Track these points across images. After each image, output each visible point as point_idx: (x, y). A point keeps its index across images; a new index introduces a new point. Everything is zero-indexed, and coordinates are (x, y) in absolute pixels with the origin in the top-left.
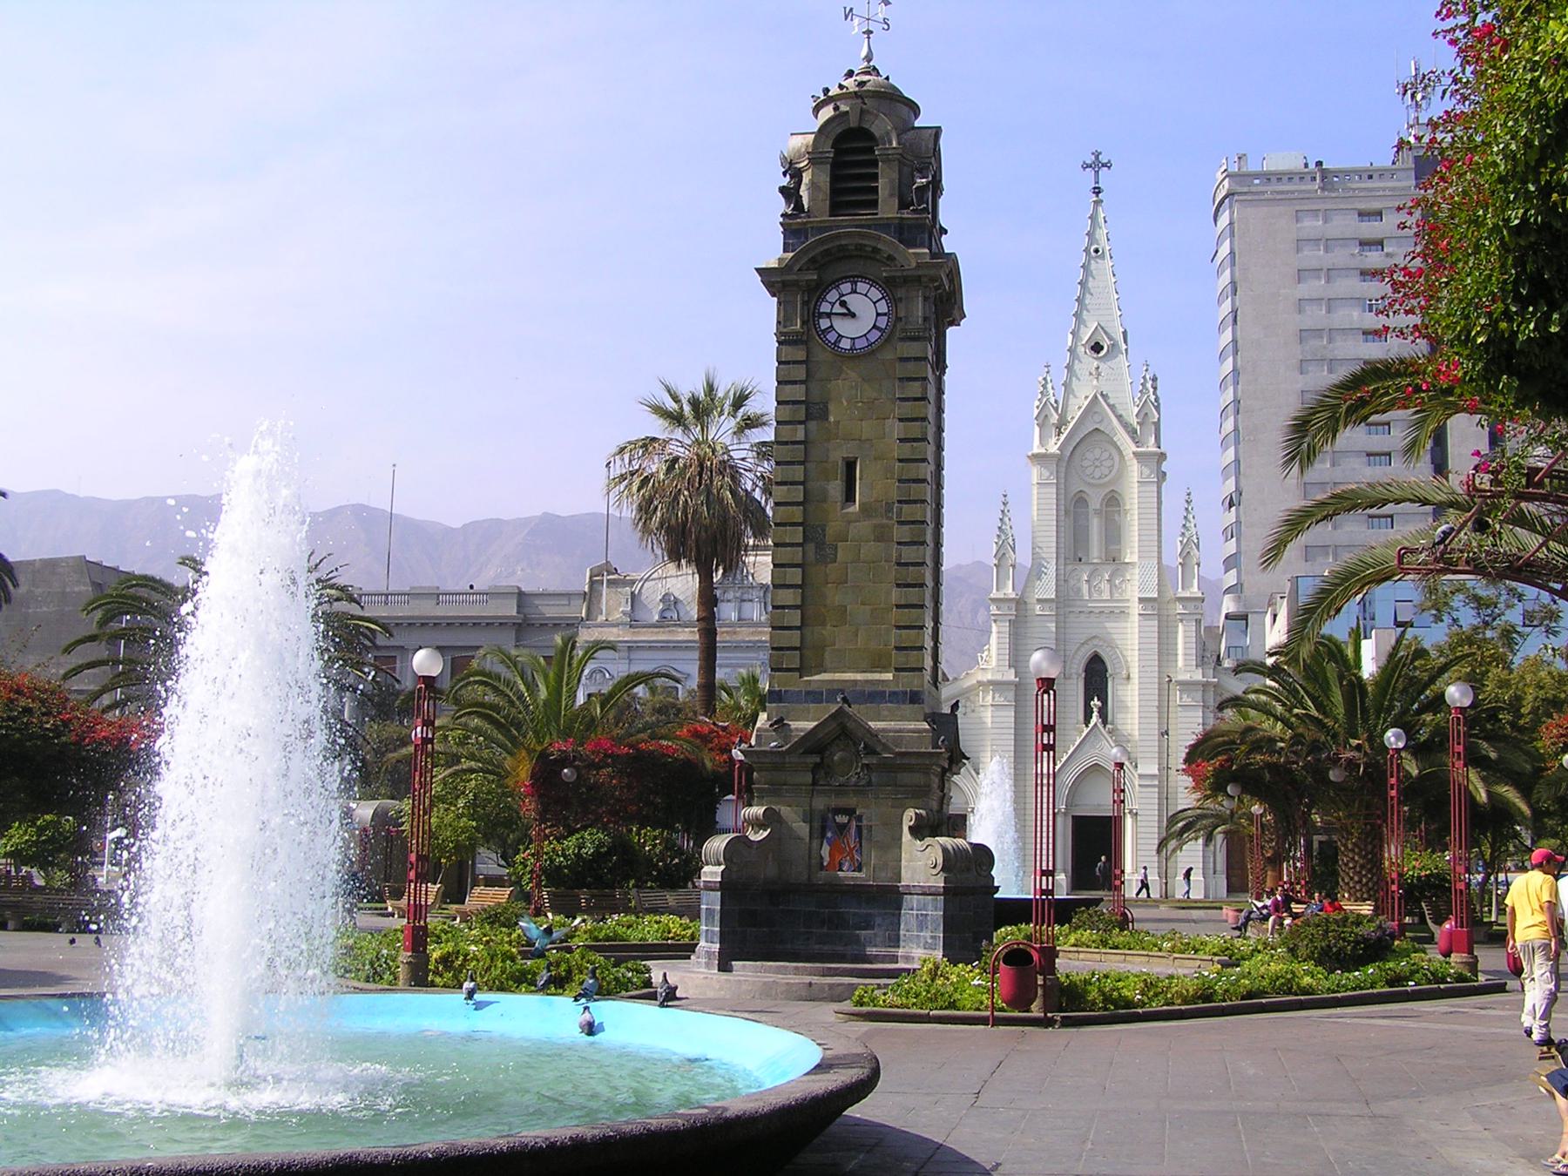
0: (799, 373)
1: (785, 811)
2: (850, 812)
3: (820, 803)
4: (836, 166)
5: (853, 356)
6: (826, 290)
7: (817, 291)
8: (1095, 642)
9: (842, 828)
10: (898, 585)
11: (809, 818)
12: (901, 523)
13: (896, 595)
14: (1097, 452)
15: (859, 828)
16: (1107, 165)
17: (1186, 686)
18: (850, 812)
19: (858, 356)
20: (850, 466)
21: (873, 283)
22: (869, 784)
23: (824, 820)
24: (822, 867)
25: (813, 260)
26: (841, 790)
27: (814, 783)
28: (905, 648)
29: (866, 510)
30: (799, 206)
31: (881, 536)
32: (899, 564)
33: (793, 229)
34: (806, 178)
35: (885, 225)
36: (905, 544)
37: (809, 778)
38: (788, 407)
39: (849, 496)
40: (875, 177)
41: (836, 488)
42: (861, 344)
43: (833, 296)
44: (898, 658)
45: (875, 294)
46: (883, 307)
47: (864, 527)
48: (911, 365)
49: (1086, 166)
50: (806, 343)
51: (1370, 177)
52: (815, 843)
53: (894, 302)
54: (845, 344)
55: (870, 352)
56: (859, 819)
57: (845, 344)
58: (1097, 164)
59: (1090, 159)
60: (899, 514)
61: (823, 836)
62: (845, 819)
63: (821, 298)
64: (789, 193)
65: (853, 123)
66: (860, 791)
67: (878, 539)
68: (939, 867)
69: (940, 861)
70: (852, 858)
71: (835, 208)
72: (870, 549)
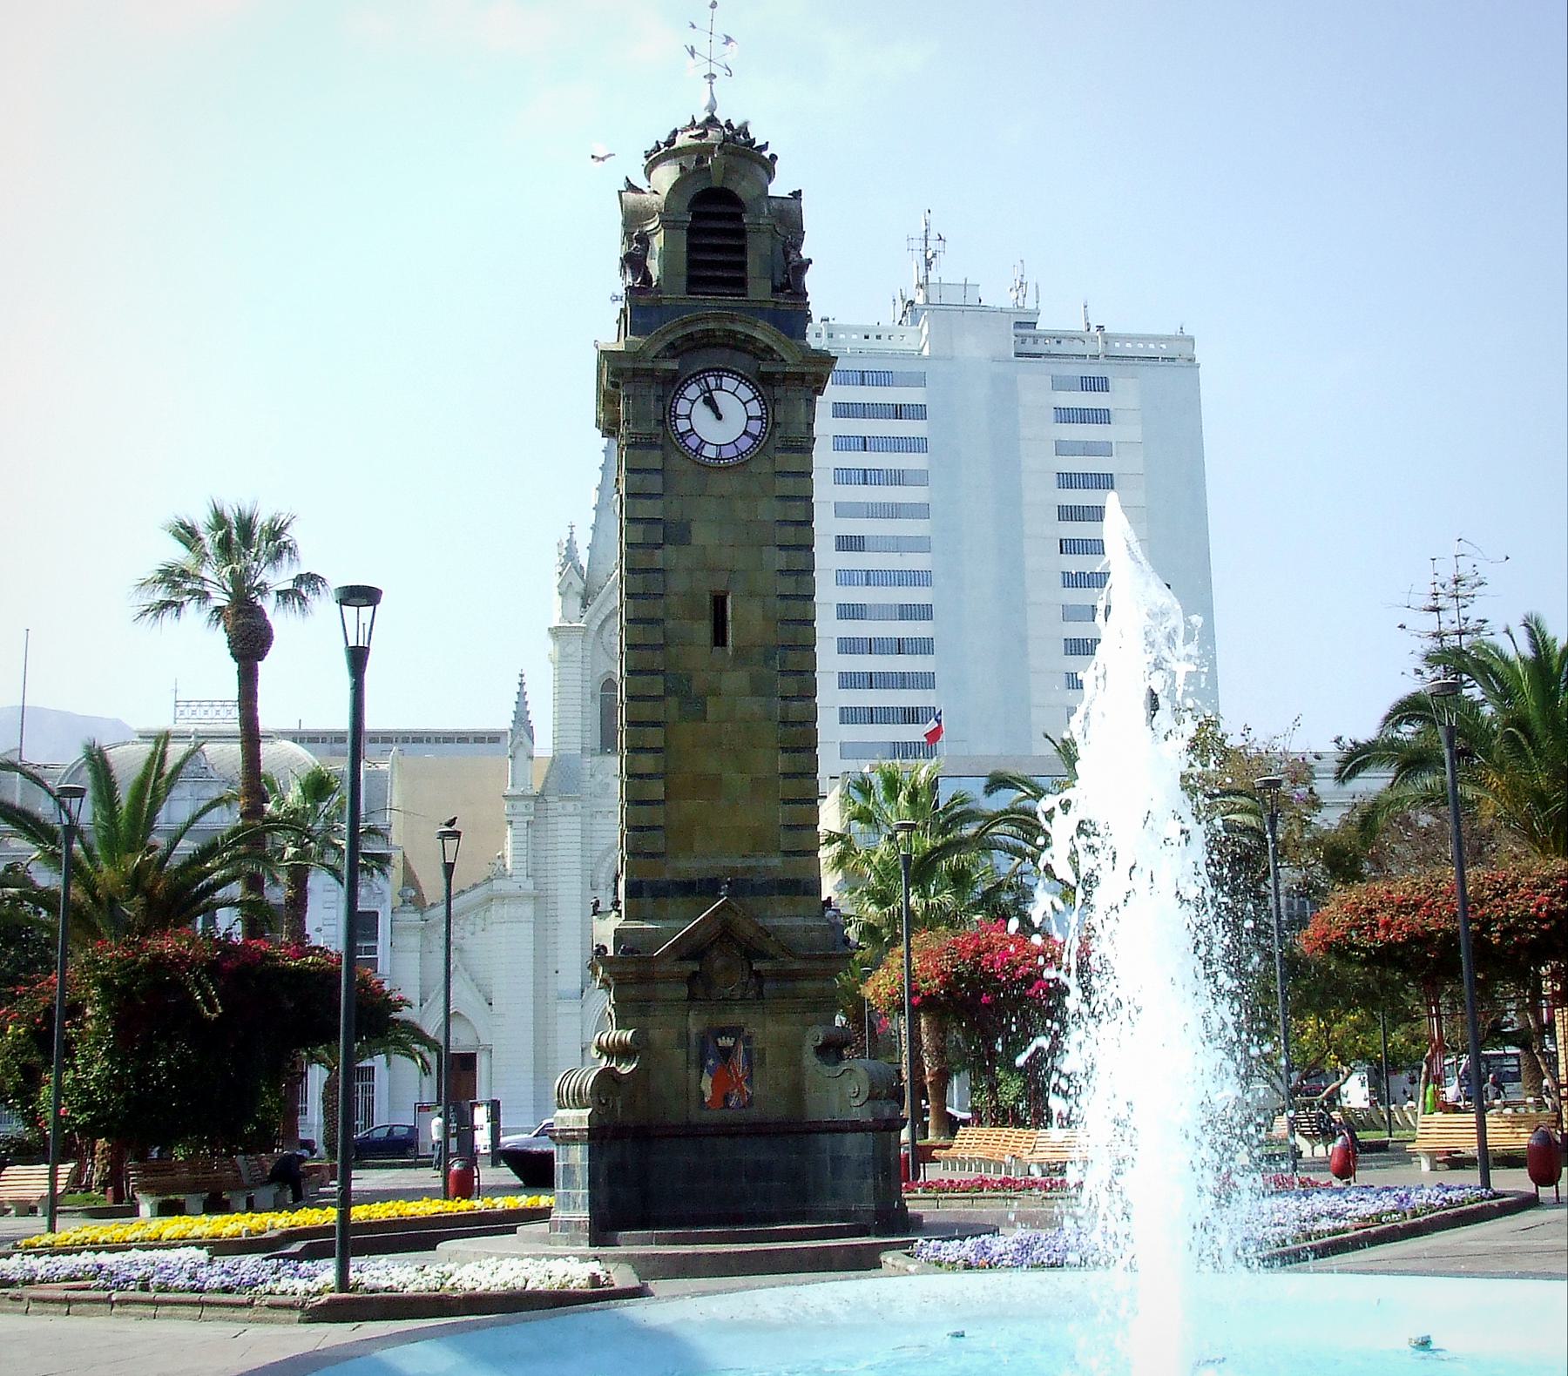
0: (655, 483)
1: (656, 1034)
4: (692, 232)
5: (719, 468)
6: (685, 384)
7: (673, 384)
9: (726, 1053)
10: (785, 750)
12: (783, 673)
13: (783, 762)
15: (748, 1053)
19: (727, 468)
20: (719, 603)
21: (743, 379)
23: (703, 1042)
25: (671, 346)
27: (692, 997)
28: (797, 827)
29: (742, 656)
30: (647, 279)
32: (784, 723)
33: (642, 305)
34: (657, 242)
35: (758, 311)
36: (792, 699)
37: (684, 991)
38: (641, 527)
39: (719, 638)
40: (742, 250)
41: (704, 630)
42: (729, 452)
43: (693, 391)
45: (746, 393)
46: (755, 409)
47: (735, 680)
48: (790, 481)
50: (662, 447)
51: (879, 337)
52: (693, 1072)
53: (768, 403)
54: (709, 452)
55: (741, 465)
56: (748, 1040)
57: (709, 452)
60: (783, 662)
61: (702, 1065)
62: (723, 1042)
63: (679, 394)
64: (634, 262)
65: (716, 184)
68: (863, 1098)
69: (866, 1088)
70: (741, 1091)
71: (694, 283)
72: (753, 706)
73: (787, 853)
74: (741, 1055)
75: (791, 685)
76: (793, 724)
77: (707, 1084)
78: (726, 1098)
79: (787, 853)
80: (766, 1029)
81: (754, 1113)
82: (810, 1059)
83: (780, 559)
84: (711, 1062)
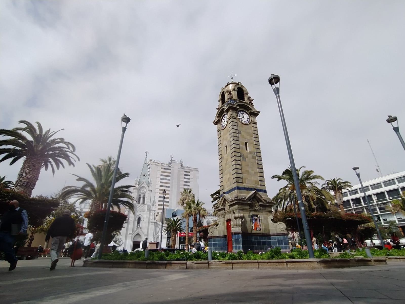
2: (257, 216)
3: (251, 214)
8: (140, 215)
9: (256, 220)
11: (250, 216)
14: (143, 189)
15: (259, 220)
16: (148, 153)
17: (152, 222)
18: (257, 216)
22: (260, 209)
24: (253, 229)
26: (255, 211)
29: (251, 153)
31: (254, 158)
44: (260, 183)
46: (248, 117)
47: (250, 156)
49: (145, 153)
54: (243, 122)
56: (259, 217)
58: (147, 153)
59: (146, 152)
61: (252, 222)
62: (256, 217)
66: (259, 211)
67: (253, 158)
70: (259, 227)
72: (252, 160)
73: (261, 185)
74: (258, 220)
75: (257, 158)
76: (259, 164)
77: (253, 225)
78: (257, 229)
79: (261, 185)
80: (262, 216)
81: (261, 232)
82: (270, 222)
83: (254, 139)
84: (254, 221)
